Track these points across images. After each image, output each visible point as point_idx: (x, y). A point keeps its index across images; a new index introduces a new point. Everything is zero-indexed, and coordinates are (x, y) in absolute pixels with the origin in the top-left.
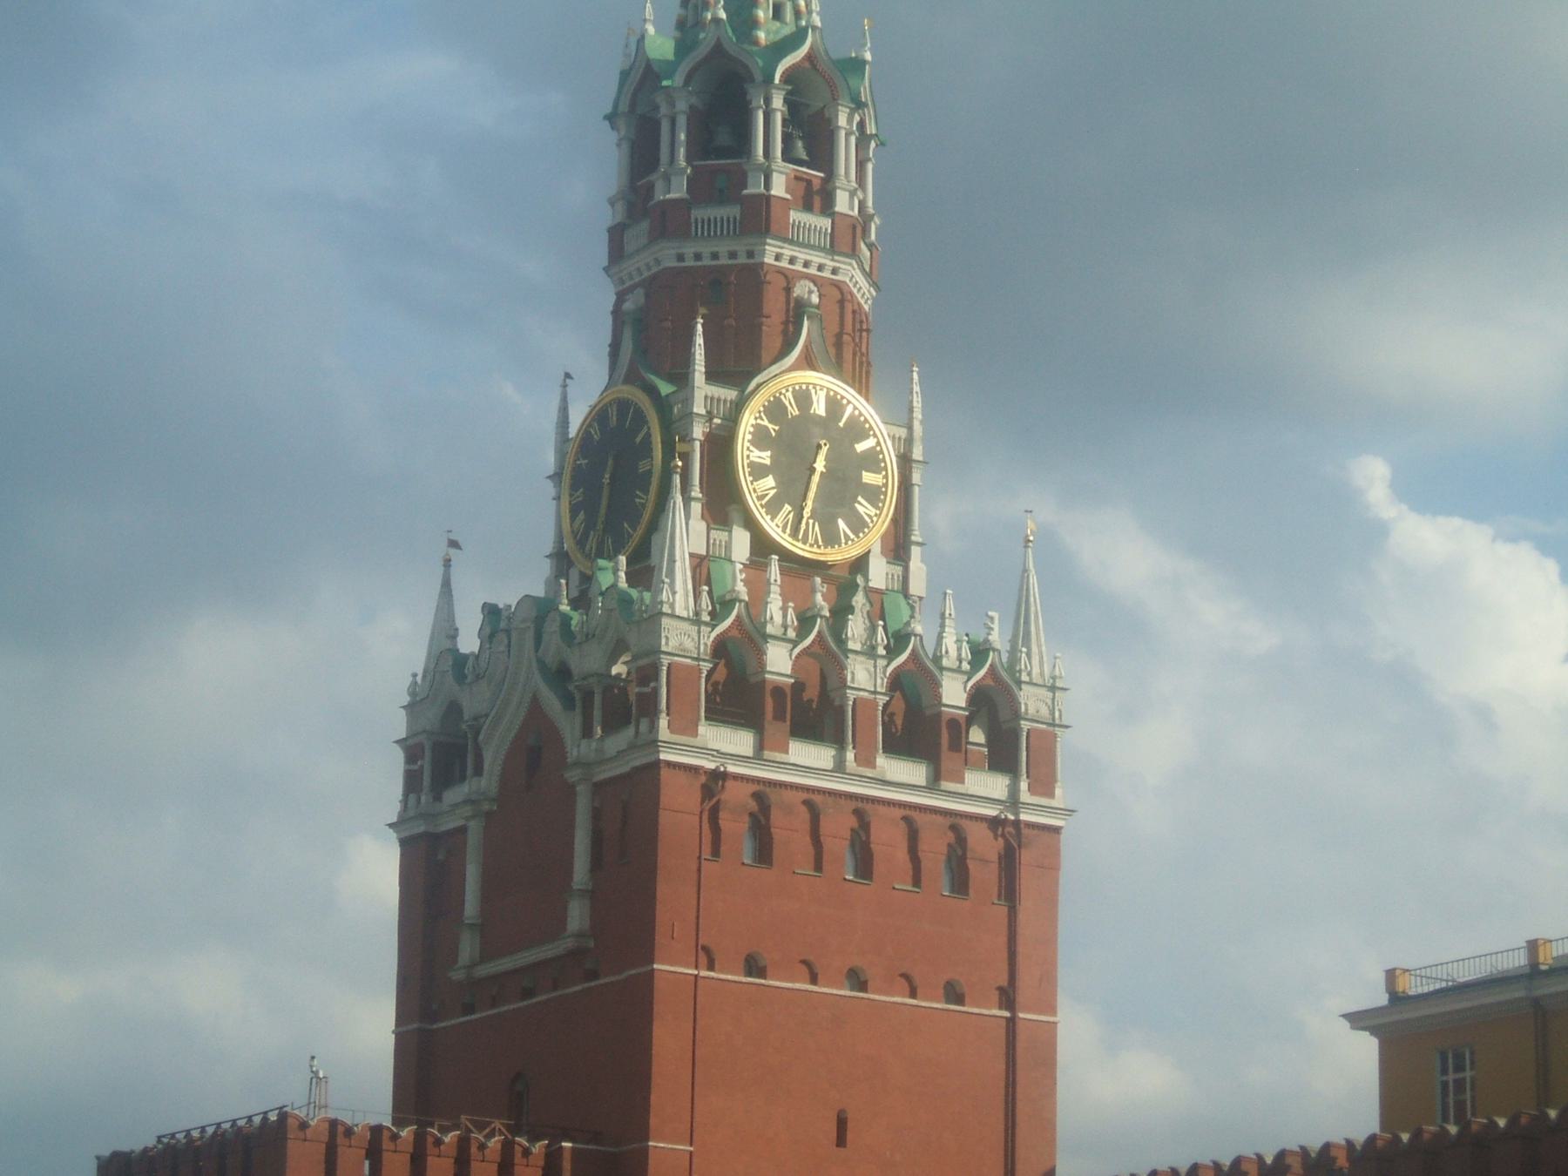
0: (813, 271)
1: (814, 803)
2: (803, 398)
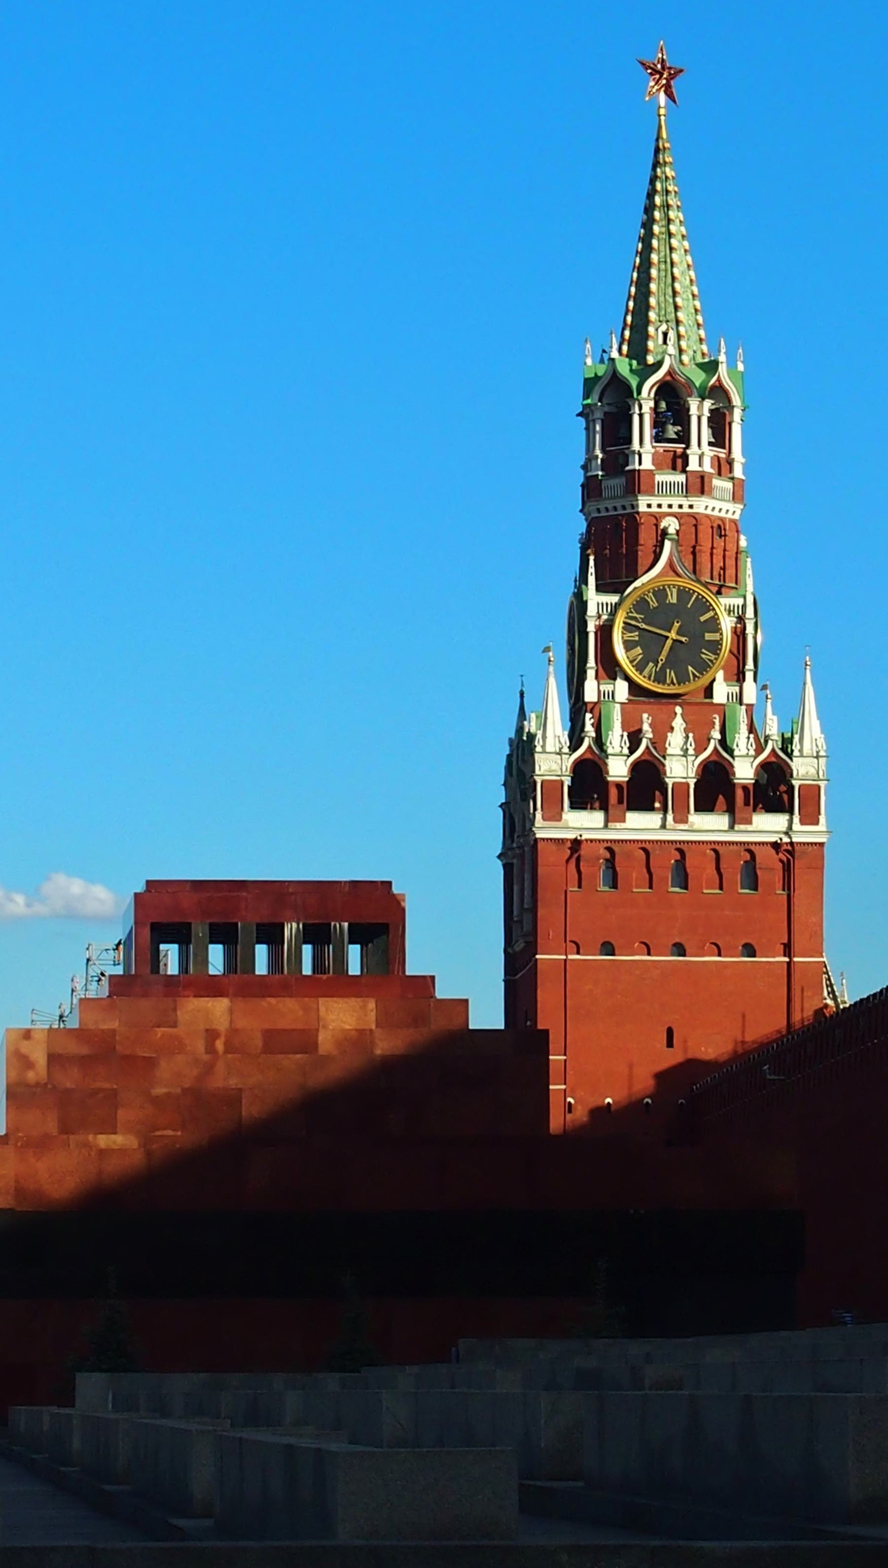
0: (675, 509)
1: (646, 848)
2: (660, 594)
